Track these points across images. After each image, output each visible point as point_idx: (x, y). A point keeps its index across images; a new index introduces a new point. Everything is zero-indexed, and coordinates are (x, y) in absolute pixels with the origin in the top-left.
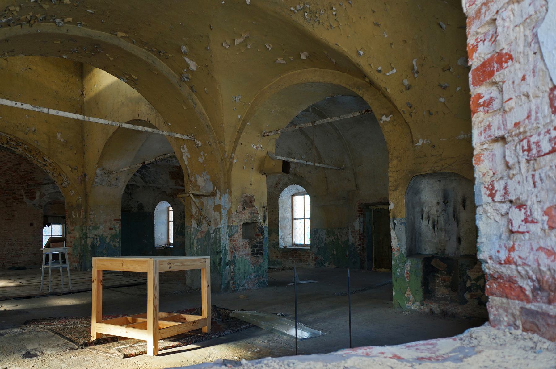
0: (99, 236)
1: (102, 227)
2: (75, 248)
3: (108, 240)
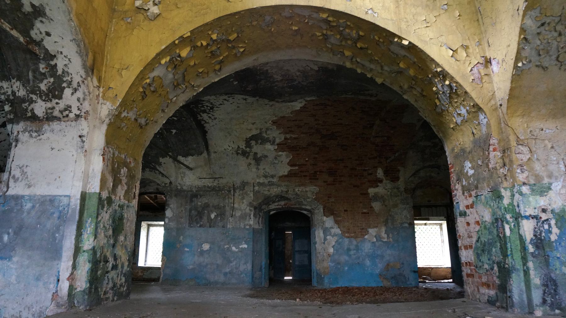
0: (553, 211)
1: (559, 187)
2: (483, 251)
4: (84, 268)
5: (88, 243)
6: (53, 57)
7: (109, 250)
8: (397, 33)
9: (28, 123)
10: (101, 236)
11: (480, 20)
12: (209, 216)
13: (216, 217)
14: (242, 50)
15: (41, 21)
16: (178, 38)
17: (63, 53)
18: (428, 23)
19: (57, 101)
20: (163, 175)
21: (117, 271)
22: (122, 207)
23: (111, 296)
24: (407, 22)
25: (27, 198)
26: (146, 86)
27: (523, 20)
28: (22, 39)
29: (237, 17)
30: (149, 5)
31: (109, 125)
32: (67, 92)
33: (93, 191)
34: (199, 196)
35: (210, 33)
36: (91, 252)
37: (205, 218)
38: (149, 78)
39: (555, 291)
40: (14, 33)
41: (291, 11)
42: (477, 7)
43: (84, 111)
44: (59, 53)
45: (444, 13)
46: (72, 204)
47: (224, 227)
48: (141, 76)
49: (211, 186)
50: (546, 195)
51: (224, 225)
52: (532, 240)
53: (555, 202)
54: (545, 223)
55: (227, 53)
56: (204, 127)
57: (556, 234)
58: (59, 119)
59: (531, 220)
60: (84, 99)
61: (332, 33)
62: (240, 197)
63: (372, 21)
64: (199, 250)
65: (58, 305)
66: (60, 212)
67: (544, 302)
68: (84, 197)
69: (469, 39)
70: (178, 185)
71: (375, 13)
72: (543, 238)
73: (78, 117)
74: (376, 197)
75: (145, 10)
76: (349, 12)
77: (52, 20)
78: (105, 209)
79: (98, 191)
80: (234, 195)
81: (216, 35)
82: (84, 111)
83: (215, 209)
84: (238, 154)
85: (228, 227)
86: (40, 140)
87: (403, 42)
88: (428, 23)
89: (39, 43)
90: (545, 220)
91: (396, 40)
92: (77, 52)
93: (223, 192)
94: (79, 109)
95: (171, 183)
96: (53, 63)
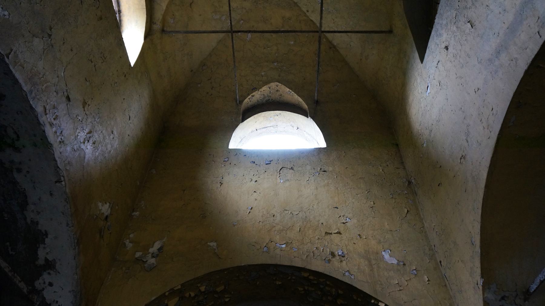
8: (373, 295)
11: (448, 285)
14: (227, 300)
15: (49, 274)
16: (168, 290)
17: (58, 302)
18: (401, 286)
24: (382, 284)
27: (483, 294)
28: (25, 290)
29: (225, 272)
30: (148, 256)
35: (199, 285)
40: (22, 285)
41: (275, 269)
42: (443, 274)
44: (55, 302)
45: (414, 278)
55: (213, 303)
61: (313, 289)
63: (349, 283)
69: (441, 304)
71: (352, 275)
75: (144, 261)
76: (328, 274)
77: (59, 272)
81: (205, 287)
87: (379, 304)
88: (401, 286)
89: (39, 292)
91: (373, 301)
92: (72, 302)
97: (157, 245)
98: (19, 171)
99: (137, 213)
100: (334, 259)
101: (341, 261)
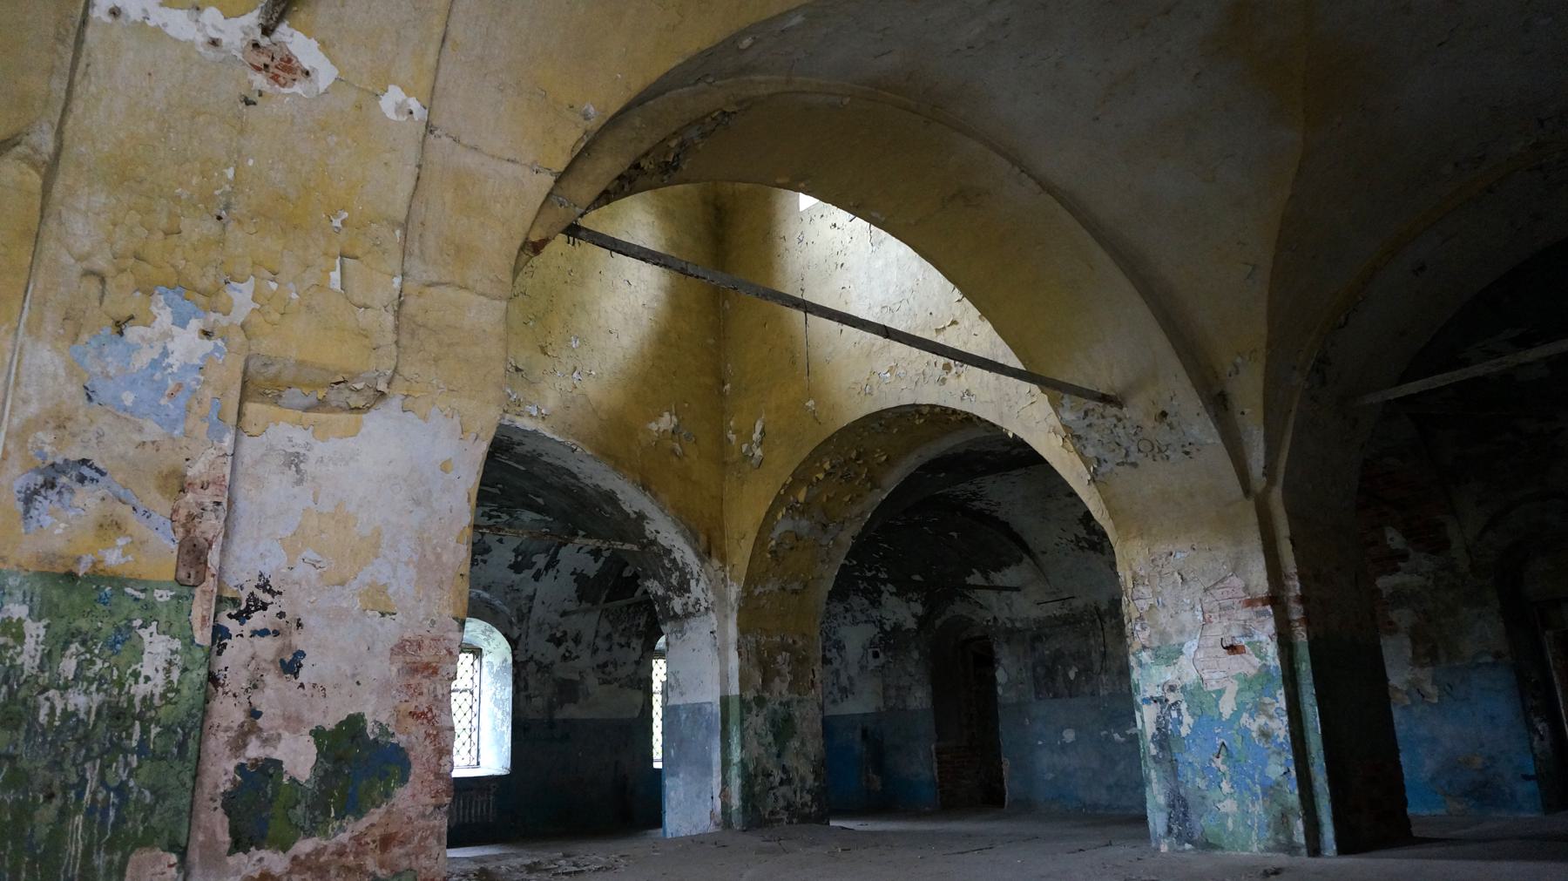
3: (1227, 707)
4: (736, 783)
5: (736, 756)
6: (670, 551)
7: (771, 761)
9: (673, 623)
10: (753, 744)
12: (1066, 675)
13: (1078, 675)
19: (688, 595)
20: (981, 607)
21: (793, 787)
22: (787, 704)
23: (785, 817)
25: (682, 707)
26: (774, 549)
31: (739, 611)
32: (693, 583)
33: (734, 693)
34: (1044, 639)
36: (739, 765)
37: (1060, 679)
38: (772, 539)
39: (1185, 815)
43: (710, 602)
46: (714, 712)
47: (1094, 695)
48: (760, 541)
49: (1060, 616)
50: (1174, 664)
51: (1093, 691)
52: (1154, 736)
53: (1187, 674)
54: (1173, 708)
56: (997, 518)
57: (1189, 725)
58: (694, 615)
59: (1153, 705)
60: (707, 589)
62: (1115, 631)
64: (1059, 743)
65: (717, 825)
66: (706, 721)
67: (1170, 830)
68: (725, 701)
70: (1006, 620)
72: (1169, 732)
73: (707, 609)
74: (1400, 597)
78: (754, 712)
79: (738, 693)
80: (1103, 629)
82: (710, 602)
83: (1075, 660)
84: (1082, 548)
85: (1102, 693)
86: (684, 640)
90: (1173, 704)
93: (1083, 624)
94: (706, 601)
95: (995, 618)
96: (672, 557)
97: (758, 428)
98: (541, 455)
99: (728, 387)
100: (949, 376)
101: (959, 376)
